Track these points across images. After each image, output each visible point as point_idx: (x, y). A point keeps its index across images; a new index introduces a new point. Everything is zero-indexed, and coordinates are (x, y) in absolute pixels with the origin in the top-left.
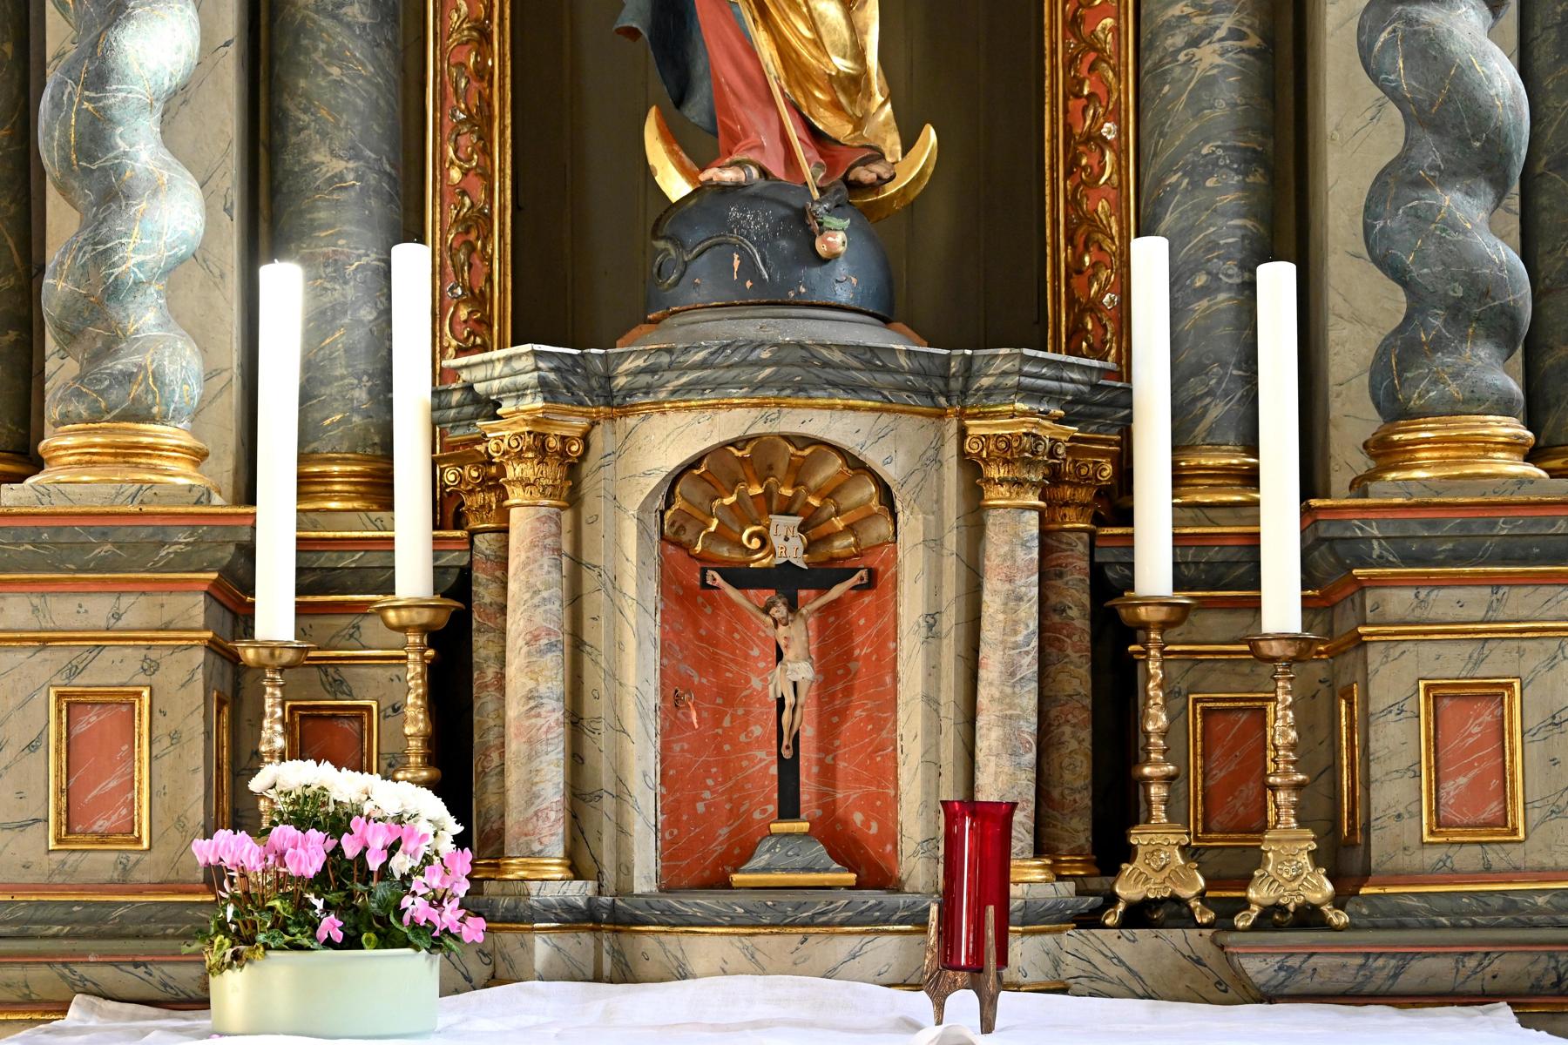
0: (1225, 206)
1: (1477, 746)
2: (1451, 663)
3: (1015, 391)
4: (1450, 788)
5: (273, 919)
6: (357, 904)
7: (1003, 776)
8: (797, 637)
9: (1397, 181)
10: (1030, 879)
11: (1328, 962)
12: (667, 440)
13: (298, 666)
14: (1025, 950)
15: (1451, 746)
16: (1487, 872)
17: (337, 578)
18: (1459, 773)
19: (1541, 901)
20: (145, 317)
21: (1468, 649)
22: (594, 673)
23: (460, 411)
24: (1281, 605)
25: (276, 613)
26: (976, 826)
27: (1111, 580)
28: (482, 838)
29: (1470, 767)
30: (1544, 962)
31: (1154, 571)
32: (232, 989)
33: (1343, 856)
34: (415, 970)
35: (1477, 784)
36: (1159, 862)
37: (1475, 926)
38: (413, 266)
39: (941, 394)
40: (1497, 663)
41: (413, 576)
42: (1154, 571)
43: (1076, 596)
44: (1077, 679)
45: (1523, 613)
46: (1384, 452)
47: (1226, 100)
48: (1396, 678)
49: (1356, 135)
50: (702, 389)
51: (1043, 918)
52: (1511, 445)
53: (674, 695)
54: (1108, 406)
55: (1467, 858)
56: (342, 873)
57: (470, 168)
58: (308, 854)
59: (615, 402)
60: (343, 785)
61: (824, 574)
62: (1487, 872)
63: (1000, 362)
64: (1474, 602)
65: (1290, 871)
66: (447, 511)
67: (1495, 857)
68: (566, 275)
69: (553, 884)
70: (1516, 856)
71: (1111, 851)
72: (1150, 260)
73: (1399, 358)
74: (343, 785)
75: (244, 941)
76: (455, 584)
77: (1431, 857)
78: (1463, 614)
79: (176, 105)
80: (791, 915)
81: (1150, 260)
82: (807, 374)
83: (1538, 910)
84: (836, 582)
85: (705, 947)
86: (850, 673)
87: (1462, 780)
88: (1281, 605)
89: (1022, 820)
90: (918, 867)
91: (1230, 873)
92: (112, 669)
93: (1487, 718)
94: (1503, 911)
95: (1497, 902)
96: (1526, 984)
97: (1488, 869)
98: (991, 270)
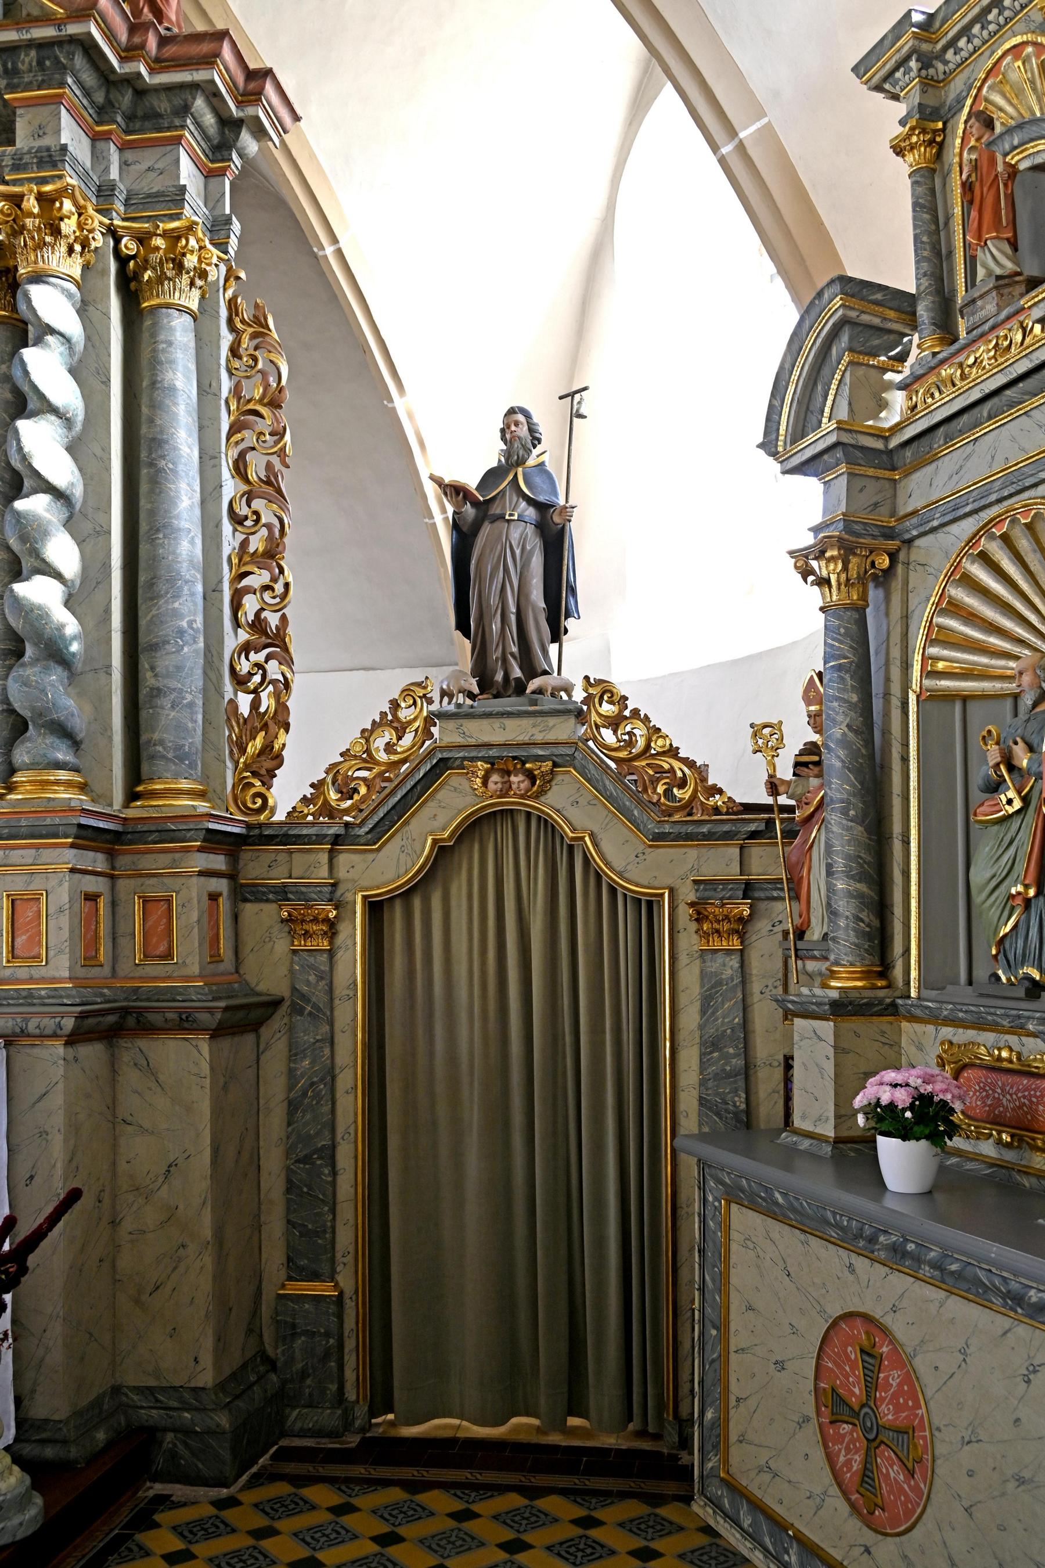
1: (30, 922)
4: (19, 941)
15: (20, 921)
16: (31, 980)
18: (22, 934)
19: (43, 993)
21: (25, 877)
29: (27, 931)
30: (10, 1024)
35: (30, 939)
37: (9, 1005)
40: (37, 884)
45: (48, 861)
52: (69, 784)
55: (23, 973)
62: (31, 980)
67: (36, 973)
70: (43, 972)
77: (7, 973)
78: (24, 861)
83: (41, 997)
87: (24, 937)
93: (35, 909)
94: (25, 998)
95: (24, 994)
96: (9, 1032)
97: (31, 978)
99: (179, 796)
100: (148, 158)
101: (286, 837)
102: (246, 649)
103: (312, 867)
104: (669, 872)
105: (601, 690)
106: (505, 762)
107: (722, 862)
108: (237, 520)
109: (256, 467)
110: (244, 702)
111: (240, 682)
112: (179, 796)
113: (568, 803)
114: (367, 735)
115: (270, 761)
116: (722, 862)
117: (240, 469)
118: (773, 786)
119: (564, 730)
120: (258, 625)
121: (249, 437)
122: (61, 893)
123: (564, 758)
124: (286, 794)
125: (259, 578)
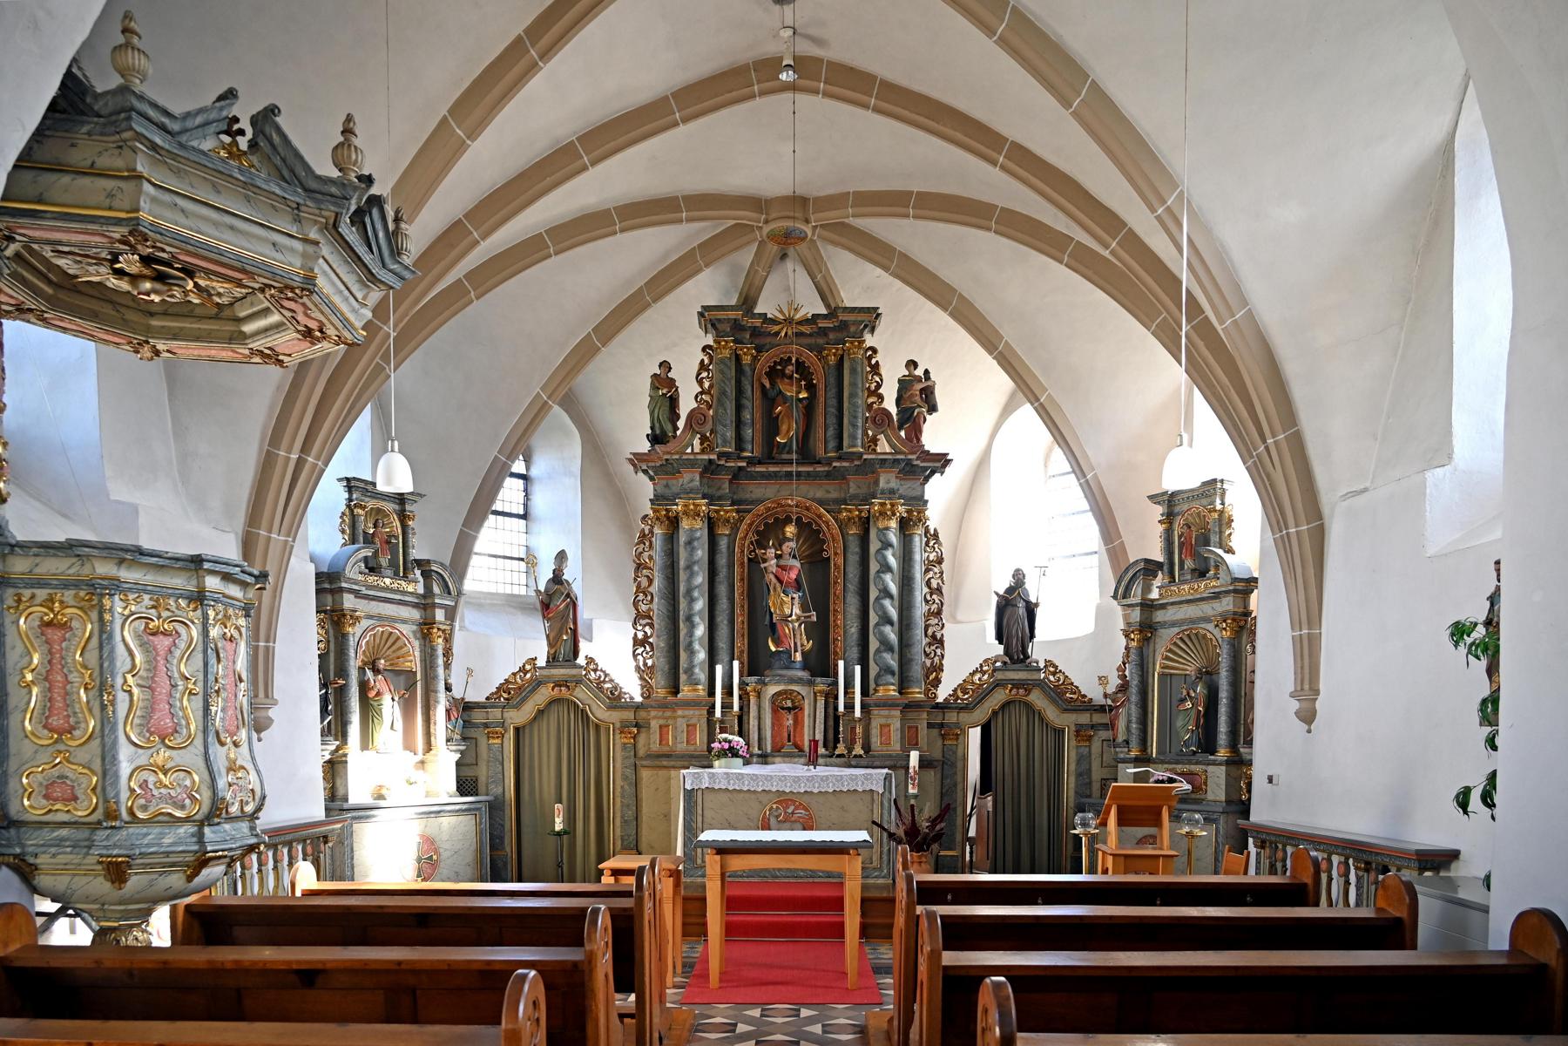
0: (854, 653)
2: (883, 721)
3: (821, 684)
5: (722, 754)
6: (733, 752)
7: (819, 736)
8: (790, 717)
9: (878, 651)
10: (821, 750)
11: (863, 762)
12: (772, 689)
13: (722, 722)
14: (820, 760)
17: (727, 706)
20: (697, 670)
22: (762, 720)
23: (742, 685)
24: (858, 713)
25: (718, 713)
26: (814, 742)
27: (836, 708)
28: (748, 744)
31: (841, 708)
32: (716, 763)
33: (867, 747)
34: (740, 761)
36: (841, 749)
38: (736, 664)
39: (811, 683)
41: (736, 708)
42: (841, 708)
43: (831, 711)
44: (831, 723)
46: (876, 691)
47: (855, 636)
48: (875, 724)
49: (874, 645)
50: (778, 683)
51: (823, 756)
53: (773, 725)
54: (836, 683)
56: (731, 748)
57: (741, 644)
58: (726, 746)
59: (765, 684)
60: (730, 737)
61: (794, 708)
63: (819, 680)
64: (885, 712)
65: (858, 750)
66: (740, 698)
68: (756, 666)
69: (756, 751)
71: (835, 747)
72: (841, 664)
73: (878, 676)
74: (730, 737)
75: (719, 757)
76: (741, 708)
79: (701, 639)
80: (790, 756)
81: (841, 664)
82: (792, 681)
84: (796, 709)
85: (777, 759)
86: (798, 722)
88: (858, 713)
89: (821, 744)
90: (806, 748)
91: (850, 750)
92: (693, 721)
98: (820, 665)
99: (917, 693)
100: (909, 484)
101: (944, 707)
102: (930, 644)
103: (952, 717)
104: (1066, 721)
105: (1049, 663)
106: (1017, 685)
107: (1084, 718)
108: (927, 602)
109: (934, 584)
110: (928, 662)
111: (927, 655)
112: (917, 693)
113: (1036, 698)
114: (972, 674)
115: (937, 682)
116: (1084, 718)
117: (928, 584)
118: (1106, 696)
119: (1034, 676)
120: (934, 636)
121: (931, 574)
122: (896, 724)
123: (1041, 684)
124: (943, 693)
125: (934, 621)
